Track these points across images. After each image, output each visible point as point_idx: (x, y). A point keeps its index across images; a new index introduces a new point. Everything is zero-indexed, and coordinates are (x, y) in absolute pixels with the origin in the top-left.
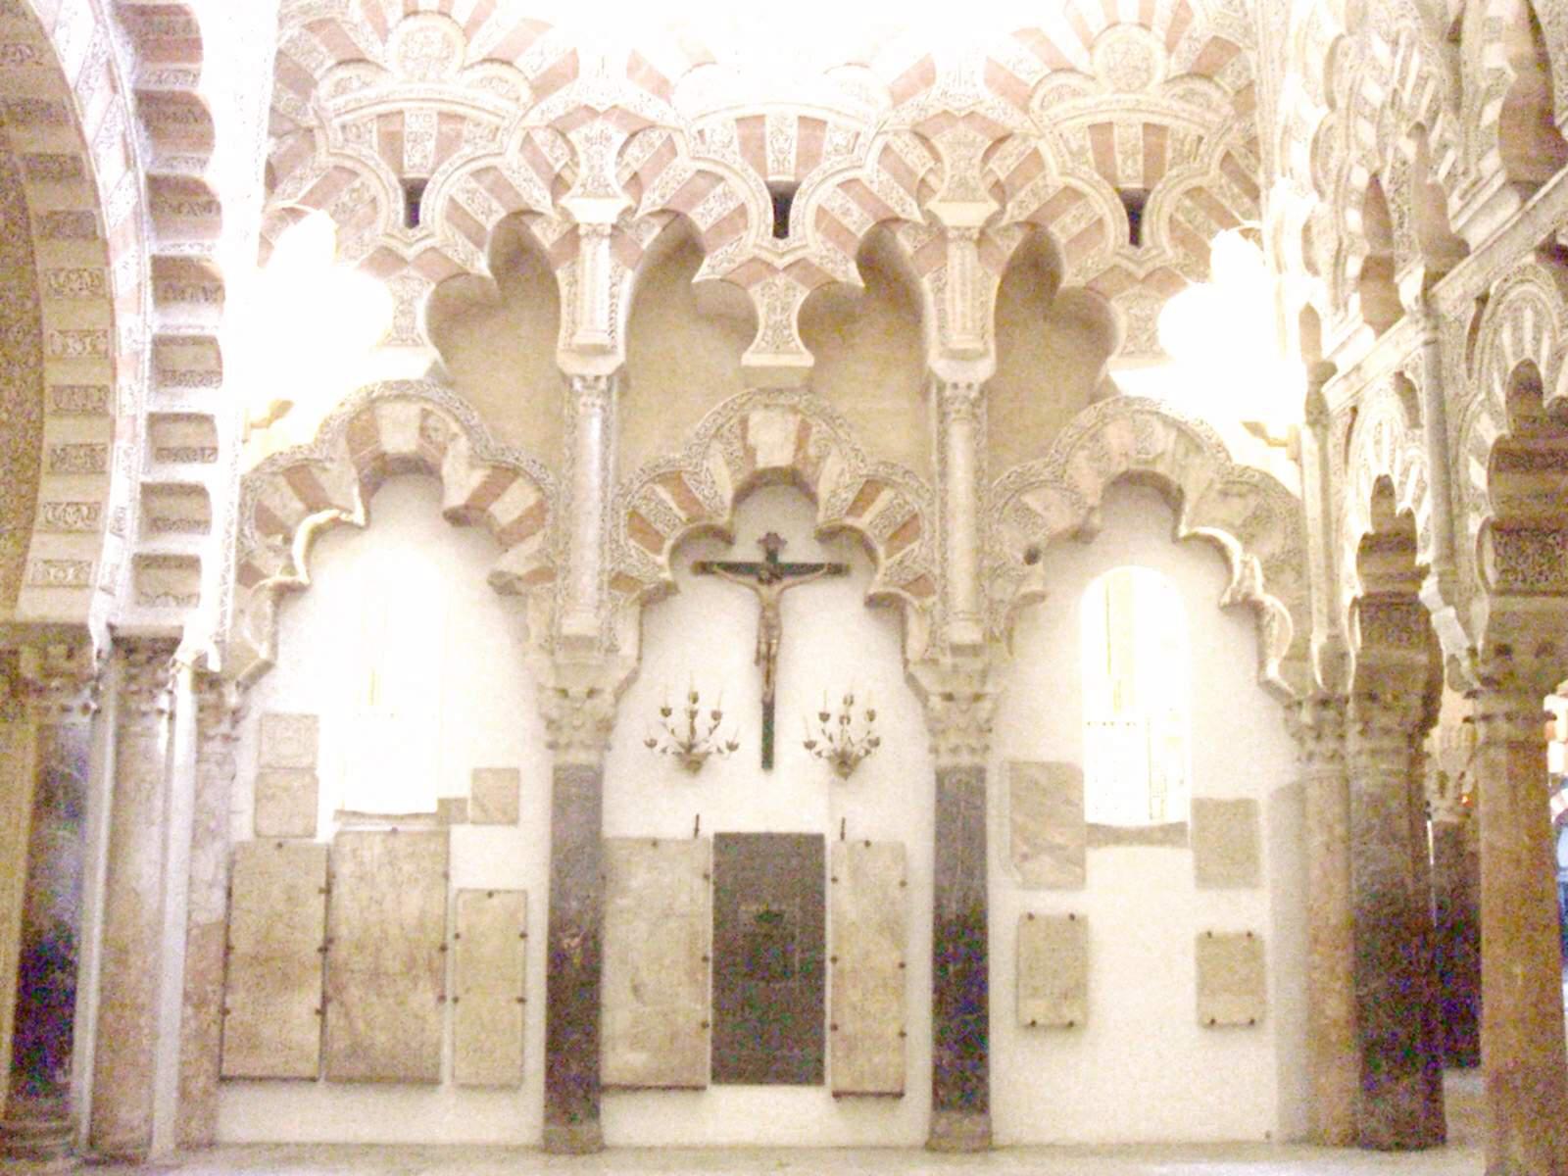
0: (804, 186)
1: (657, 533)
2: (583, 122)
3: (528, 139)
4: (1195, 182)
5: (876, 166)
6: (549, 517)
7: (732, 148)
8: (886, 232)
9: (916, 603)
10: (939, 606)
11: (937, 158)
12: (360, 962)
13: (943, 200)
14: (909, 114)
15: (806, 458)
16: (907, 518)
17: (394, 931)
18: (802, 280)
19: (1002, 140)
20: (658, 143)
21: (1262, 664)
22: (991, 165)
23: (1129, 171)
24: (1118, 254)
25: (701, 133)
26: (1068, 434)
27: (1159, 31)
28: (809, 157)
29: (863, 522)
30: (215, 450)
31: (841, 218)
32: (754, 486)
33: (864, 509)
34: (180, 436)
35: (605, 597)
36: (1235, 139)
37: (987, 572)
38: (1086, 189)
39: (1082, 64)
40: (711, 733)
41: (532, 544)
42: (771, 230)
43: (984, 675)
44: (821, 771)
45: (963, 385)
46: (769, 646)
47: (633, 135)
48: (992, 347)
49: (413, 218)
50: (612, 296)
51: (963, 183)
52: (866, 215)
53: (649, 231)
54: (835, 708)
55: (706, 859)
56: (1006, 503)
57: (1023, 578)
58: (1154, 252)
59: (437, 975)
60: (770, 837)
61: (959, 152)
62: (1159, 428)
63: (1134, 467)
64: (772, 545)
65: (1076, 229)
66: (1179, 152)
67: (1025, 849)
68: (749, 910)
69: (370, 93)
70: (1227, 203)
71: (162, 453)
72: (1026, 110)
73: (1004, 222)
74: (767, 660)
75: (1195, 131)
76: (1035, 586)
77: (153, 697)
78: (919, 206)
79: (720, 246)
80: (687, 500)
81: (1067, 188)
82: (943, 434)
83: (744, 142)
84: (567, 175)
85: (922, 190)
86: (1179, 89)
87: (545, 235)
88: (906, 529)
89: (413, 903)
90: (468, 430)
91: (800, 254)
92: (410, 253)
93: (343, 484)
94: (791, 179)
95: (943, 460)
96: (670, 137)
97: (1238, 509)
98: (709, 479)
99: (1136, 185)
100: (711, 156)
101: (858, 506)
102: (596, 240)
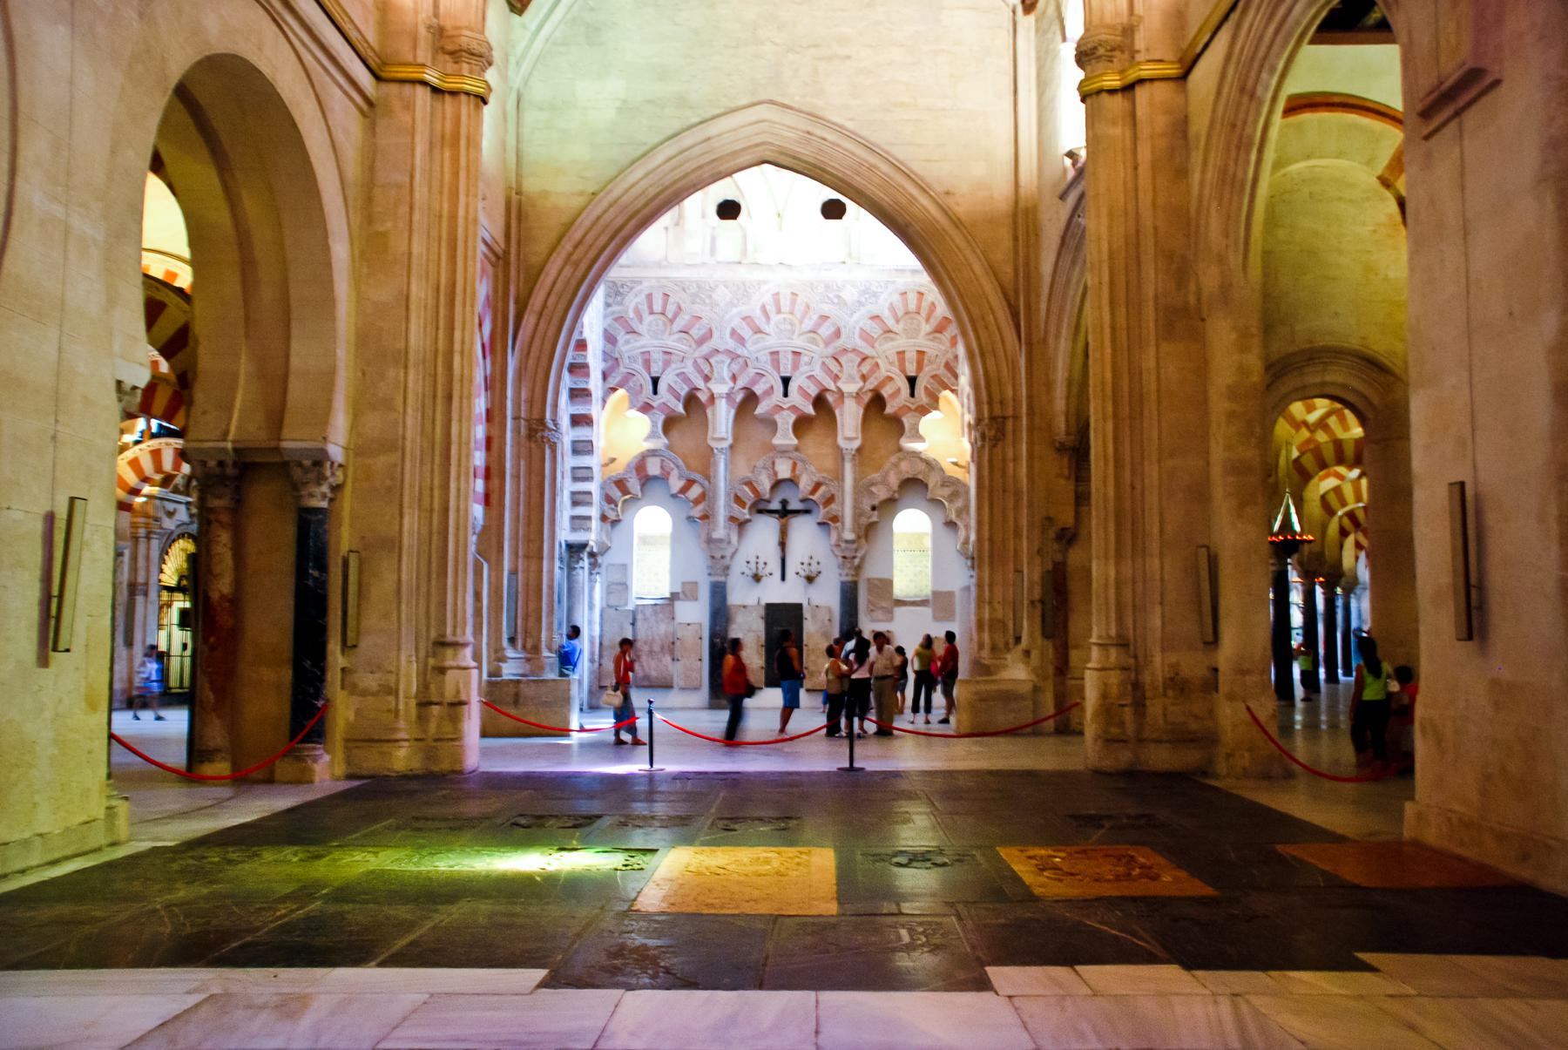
3: (695, 361)
6: (707, 498)
12: (646, 648)
13: (844, 383)
14: (830, 351)
17: (657, 638)
19: (864, 360)
26: (887, 466)
27: (924, 313)
28: (796, 366)
29: (814, 498)
30: (592, 478)
32: (777, 484)
34: (580, 474)
36: (950, 356)
37: (858, 514)
38: (893, 376)
41: (701, 507)
43: (856, 550)
44: (802, 582)
48: (860, 436)
49: (655, 392)
54: (806, 561)
55: (762, 612)
57: (869, 517)
59: (672, 652)
60: (784, 604)
61: (850, 364)
62: (918, 461)
64: (784, 503)
65: (890, 392)
67: (872, 608)
68: (777, 629)
69: (638, 344)
70: (945, 380)
71: (575, 479)
74: (783, 545)
75: (936, 353)
76: (874, 519)
77: (578, 562)
80: (754, 490)
82: (843, 466)
84: (709, 374)
85: (836, 378)
86: (931, 337)
87: (703, 397)
88: (830, 500)
89: (663, 628)
90: (678, 467)
92: (655, 404)
93: (634, 485)
97: (947, 491)
99: (913, 374)
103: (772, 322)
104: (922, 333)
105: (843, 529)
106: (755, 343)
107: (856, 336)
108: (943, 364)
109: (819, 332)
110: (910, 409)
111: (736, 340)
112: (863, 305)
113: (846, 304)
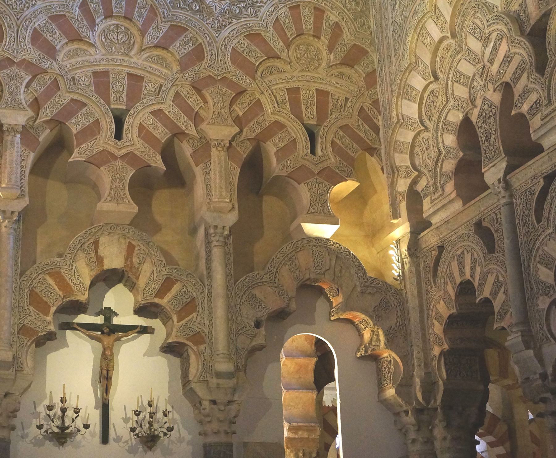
0: (132, 112)
1: (46, 302)
2: (6, 67)
4: (344, 122)
5: (172, 103)
7: (90, 88)
8: (176, 139)
9: (195, 348)
10: (208, 350)
11: (205, 101)
13: (208, 124)
15: (132, 263)
16: (189, 300)
18: (132, 165)
20: (49, 83)
21: (381, 388)
22: (234, 106)
23: (309, 115)
24: (304, 159)
25: (73, 78)
29: (163, 302)
31: (151, 130)
33: (165, 294)
35: (15, 339)
38: (287, 123)
39: (284, 55)
40: (73, 421)
42: (113, 135)
45: (220, 226)
46: (108, 371)
47: (34, 77)
48: (236, 206)
50: (22, 167)
51: (220, 115)
52: (166, 130)
53: (43, 130)
56: (244, 294)
58: (323, 159)
63: (312, 276)
65: (281, 145)
66: (335, 106)
70: (362, 135)
72: (254, 78)
73: (242, 138)
78: (195, 128)
79: (85, 142)
81: (276, 122)
83: (97, 86)
85: (197, 119)
86: (335, 72)
91: (129, 149)
94: (124, 107)
95: (209, 269)
96: (55, 78)
98: (76, 274)
100: (79, 91)
101: (161, 293)
102: (13, 134)
103: (99, 29)
104: (324, 64)
105: (212, 355)
106: (68, 56)
107: (228, 59)
108: (356, 112)
109: (171, 49)
110: (312, 173)
111: (40, 48)
112: (237, 18)
113: (211, 13)
